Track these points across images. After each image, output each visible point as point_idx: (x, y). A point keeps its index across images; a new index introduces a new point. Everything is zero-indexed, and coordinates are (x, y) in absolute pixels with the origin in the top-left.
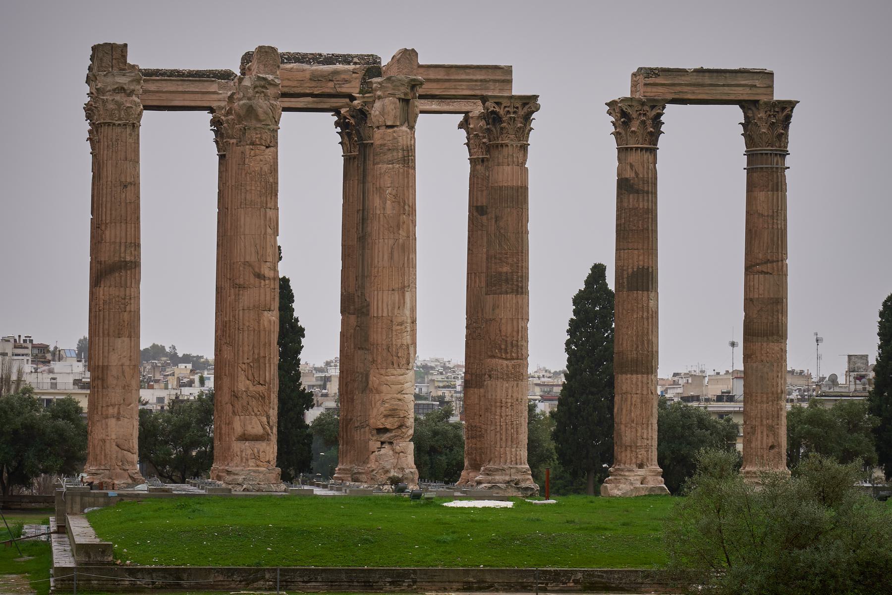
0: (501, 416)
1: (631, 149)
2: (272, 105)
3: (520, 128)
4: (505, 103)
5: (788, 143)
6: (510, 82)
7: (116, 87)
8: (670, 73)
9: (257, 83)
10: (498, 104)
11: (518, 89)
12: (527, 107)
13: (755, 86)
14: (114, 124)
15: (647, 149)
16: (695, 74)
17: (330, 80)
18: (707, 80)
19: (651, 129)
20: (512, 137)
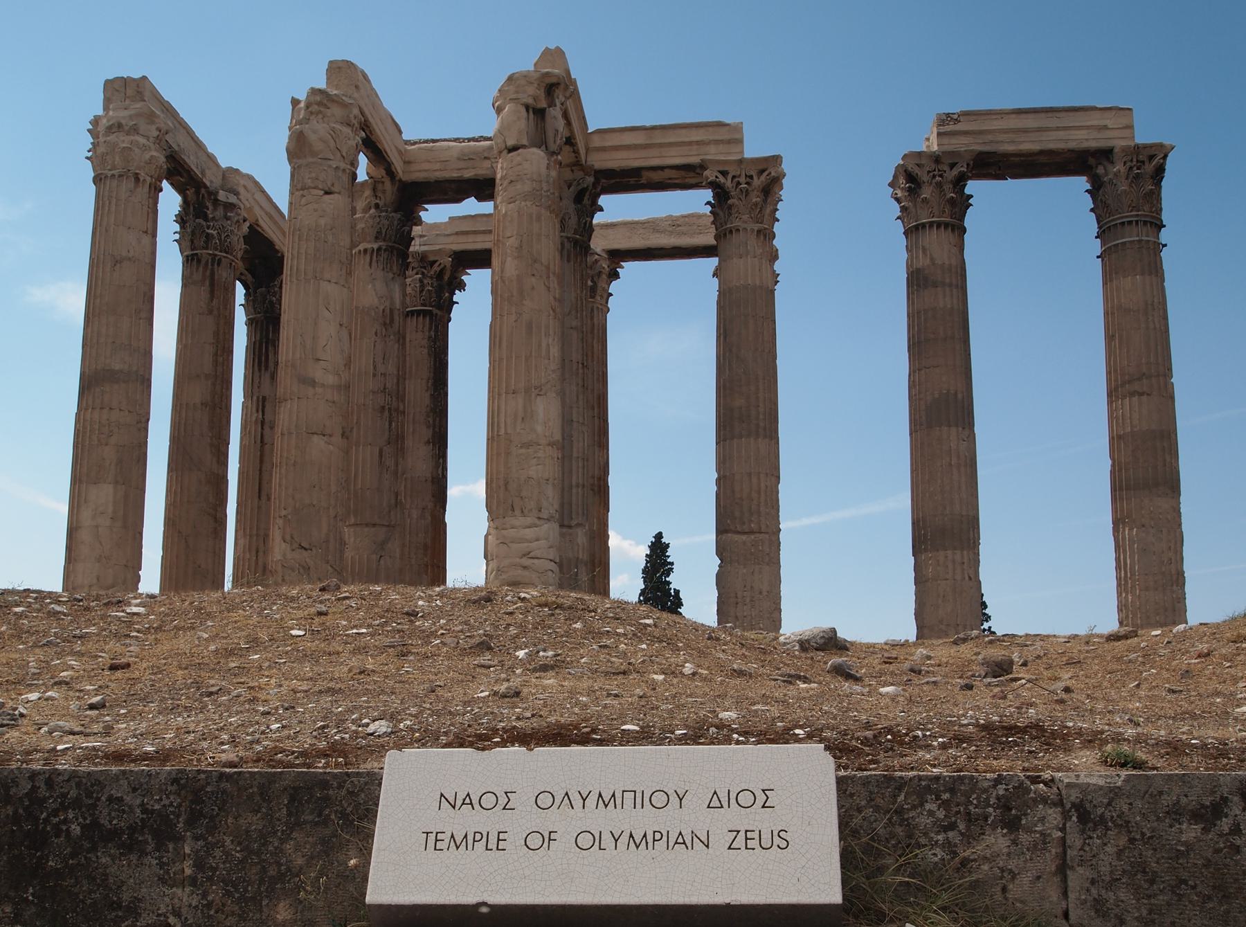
0: (737, 617)
1: (923, 225)
2: (333, 130)
3: (756, 204)
4: (733, 171)
5: (1161, 209)
6: (739, 142)
7: (111, 123)
8: (975, 117)
9: (312, 99)
10: (724, 173)
11: (753, 149)
12: (766, 173)
13: (1106, 127)
14: (106, 177)
15: (946, 225)
16: (1014, 116)
17: (485, 158)
18: (1030, 122)
19: (952, 195)
20: (745, 217)
